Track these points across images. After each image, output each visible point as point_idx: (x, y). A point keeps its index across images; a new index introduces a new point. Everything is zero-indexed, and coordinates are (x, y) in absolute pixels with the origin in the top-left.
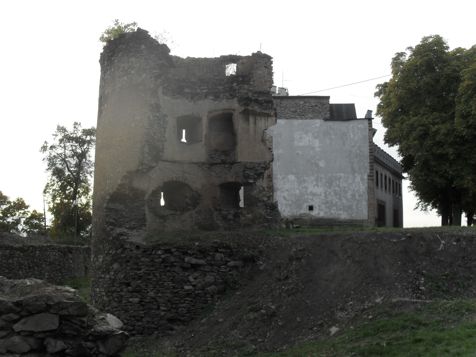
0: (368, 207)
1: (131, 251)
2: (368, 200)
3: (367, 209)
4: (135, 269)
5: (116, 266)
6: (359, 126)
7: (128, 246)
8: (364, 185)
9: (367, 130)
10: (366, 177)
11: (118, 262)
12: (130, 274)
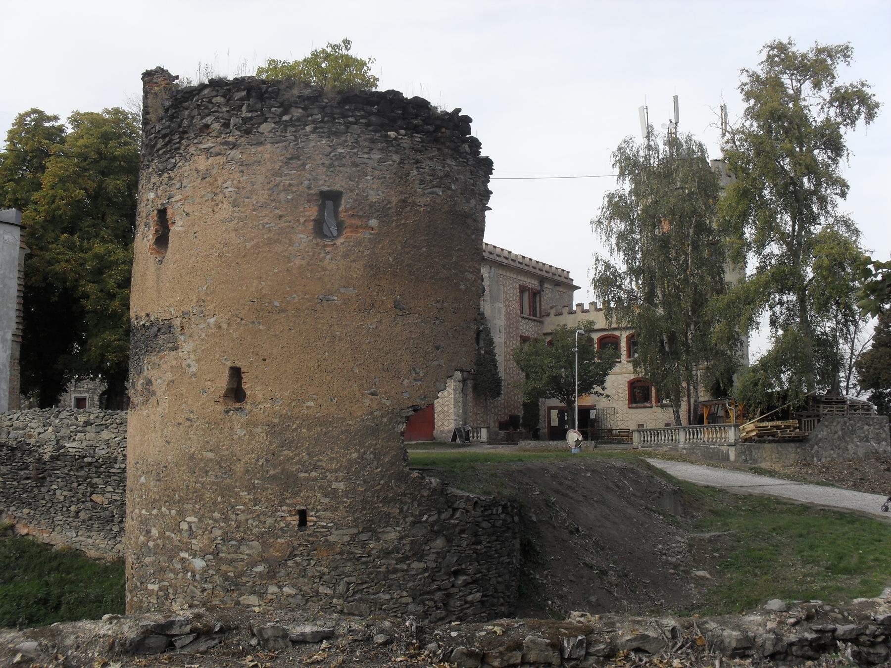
0: (10, 393)
1: (467, 511)
2: (11, 380)
3: (7, 398)
4: (473, 544)
5: (439, 543)
6: (6, 237)
7: (463, 505)
8: (5, 352)
9: (18, 248)
10: (9, 336)
11: (444, 535)
12: (467, 552)
